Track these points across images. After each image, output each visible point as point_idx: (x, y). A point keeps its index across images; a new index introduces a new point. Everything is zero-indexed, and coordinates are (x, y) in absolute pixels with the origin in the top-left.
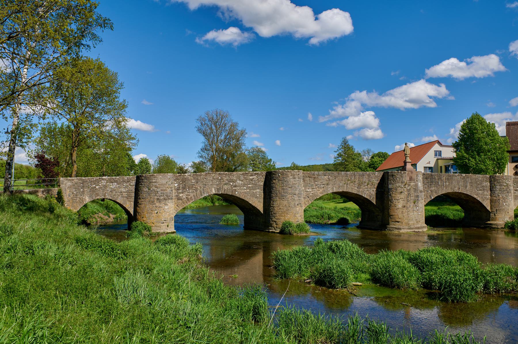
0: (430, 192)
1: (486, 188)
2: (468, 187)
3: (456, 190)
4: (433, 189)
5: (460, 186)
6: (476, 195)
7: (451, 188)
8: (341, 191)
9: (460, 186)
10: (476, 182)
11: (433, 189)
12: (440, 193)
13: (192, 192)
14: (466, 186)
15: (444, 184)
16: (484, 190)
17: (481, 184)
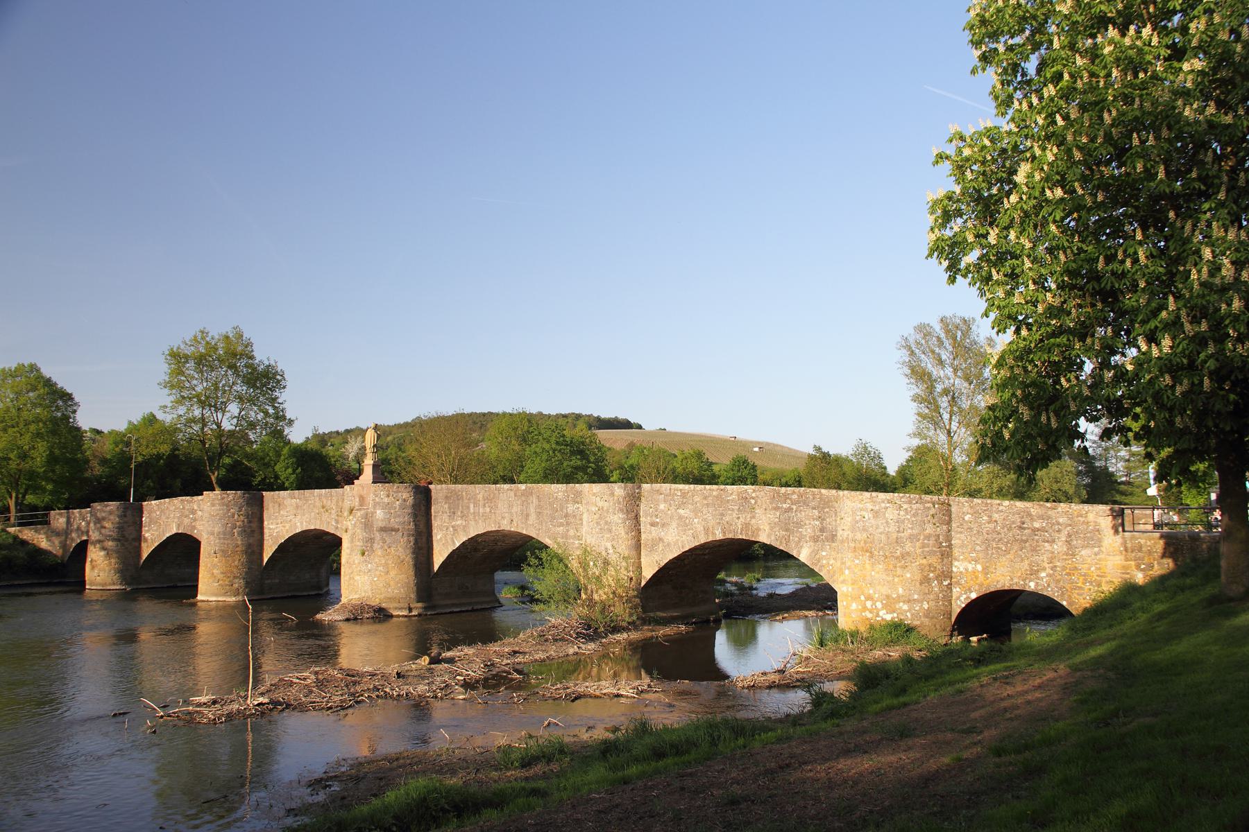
0: (451, 529)
1: (572, 520)
2: (533, 517)
3: (506, 526)
4: (459, 522)
5: (515, 515)
6: (549, 538)
7: (495, 522)
8: (313, 528)
9: (515, 515)
10: (551, 504)
11: (459, 522)
12: (472, 535)
13: (156, 530)
14: (527, 515)
15: (481, 510)
16: (568, 524)
17: (562, 510)
